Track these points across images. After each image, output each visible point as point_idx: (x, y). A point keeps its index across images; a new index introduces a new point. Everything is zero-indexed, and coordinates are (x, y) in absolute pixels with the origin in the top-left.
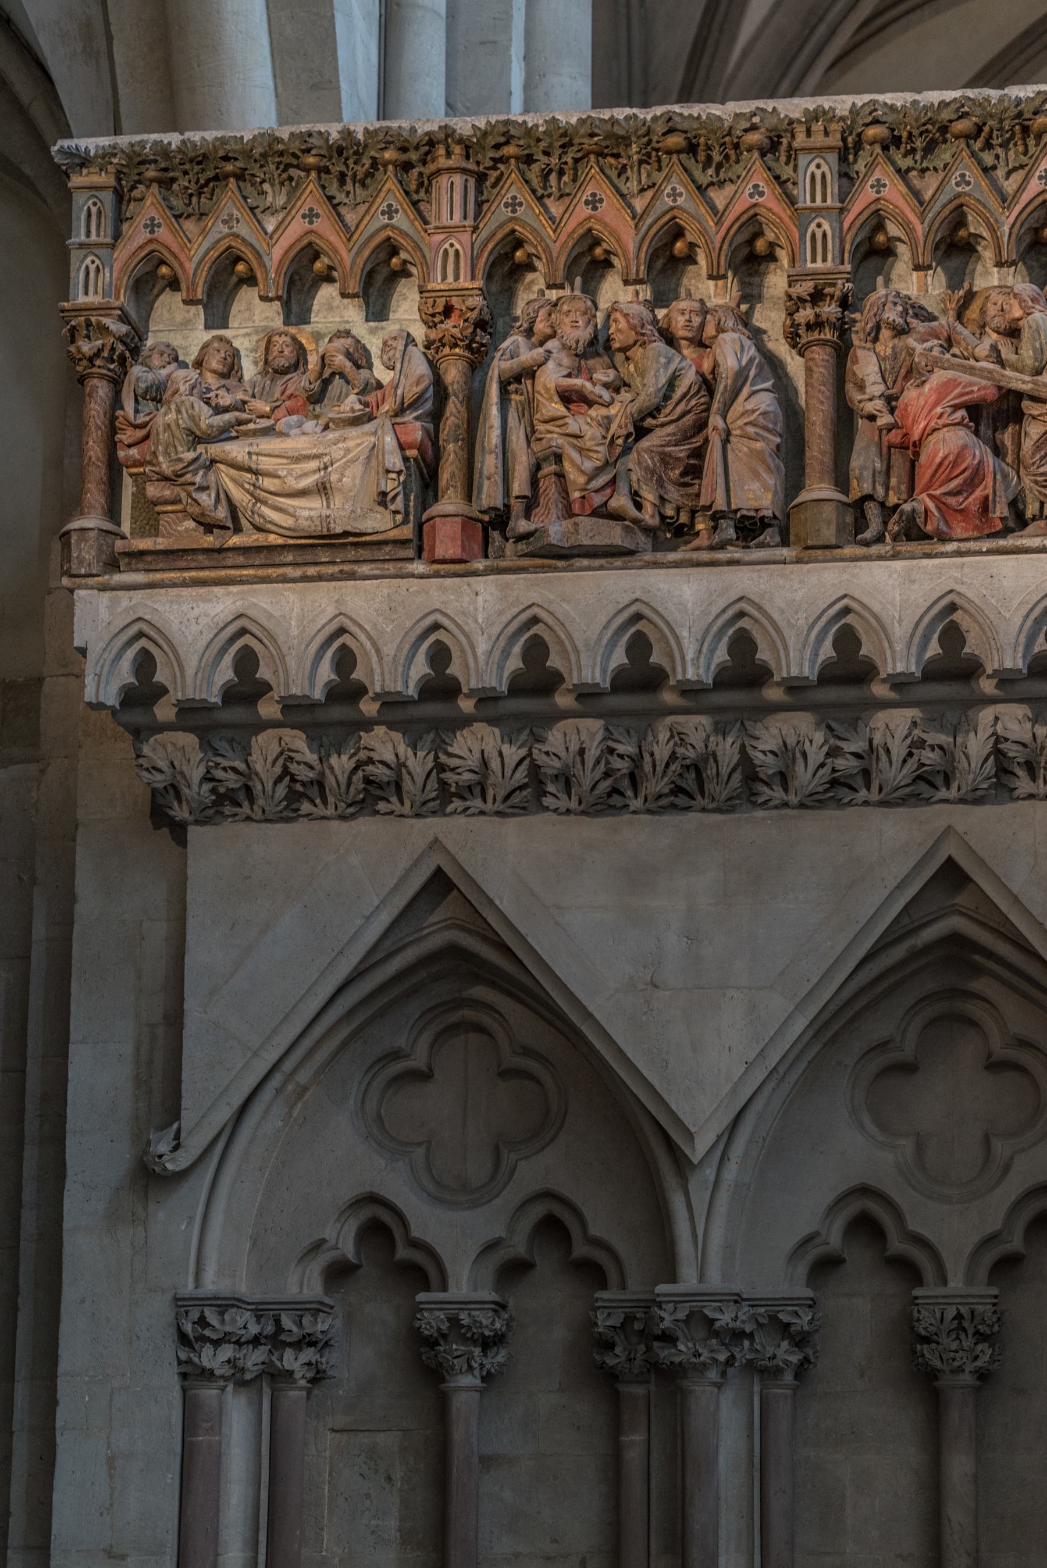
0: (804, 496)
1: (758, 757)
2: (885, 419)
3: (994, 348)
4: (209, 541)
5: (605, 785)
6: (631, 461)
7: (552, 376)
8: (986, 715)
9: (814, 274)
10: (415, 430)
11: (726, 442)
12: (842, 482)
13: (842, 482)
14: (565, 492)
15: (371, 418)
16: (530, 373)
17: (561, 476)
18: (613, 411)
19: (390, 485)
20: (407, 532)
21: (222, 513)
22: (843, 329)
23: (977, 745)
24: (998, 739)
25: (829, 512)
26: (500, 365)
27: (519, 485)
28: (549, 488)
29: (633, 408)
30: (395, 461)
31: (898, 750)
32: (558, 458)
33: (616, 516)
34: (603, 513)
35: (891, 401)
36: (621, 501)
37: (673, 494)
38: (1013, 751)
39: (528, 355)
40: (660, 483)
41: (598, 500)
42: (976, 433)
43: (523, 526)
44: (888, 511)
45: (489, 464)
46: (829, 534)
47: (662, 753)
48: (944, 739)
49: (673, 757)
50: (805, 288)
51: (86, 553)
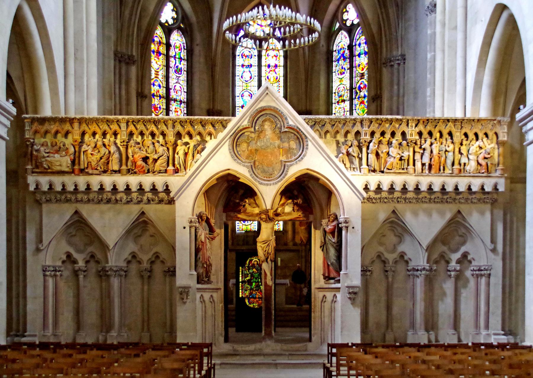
0: (121, 168)
1: (117, 198)
2: (132, 159)
3: (146, 150)
4: (45, 171)
5: (98, 201)
6: (100, 163)
7: (90, 152)
8: (146, 194)
9: (123, 139)
10: (72, 157)
11: (112, 160)
12: (127, 166)
13: (127, 166)
14: (91, 166)
15: (66, 155)
16: (87, 151)
17: (91, 164)
18: (98, 156)
19: (69, 165)
20: (71, 170)
21: (47, 167)
22: (127, 146)
23: (145, 198)
24: (148, 197)
25: (125, 170)
26: (83, 150)
27: (86, 166)
28: (90, 166)
29: (100, 156)
30: (70, 162)
31: (135, 198)
32: (91, 162)
33: (98, 170)
34: (96, 169)
35: (133, 156)
36: (99, 168)
37: (106, 167)
38: (150, 199)
39: (87, 149)
40: (104, 165)
41: (96, 168)
42: (143, 161)
43: (86, 171)
44: (132, 170)
45: (82, 163)
46: (125, 173)
47: (105, 198)
48: (141, 197)
49: (106, 198)
50: (122, 141)
51: (29, 171)
